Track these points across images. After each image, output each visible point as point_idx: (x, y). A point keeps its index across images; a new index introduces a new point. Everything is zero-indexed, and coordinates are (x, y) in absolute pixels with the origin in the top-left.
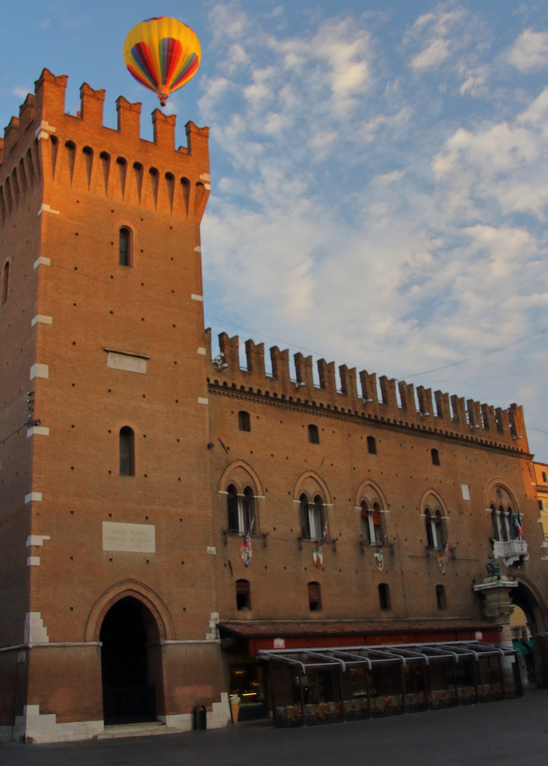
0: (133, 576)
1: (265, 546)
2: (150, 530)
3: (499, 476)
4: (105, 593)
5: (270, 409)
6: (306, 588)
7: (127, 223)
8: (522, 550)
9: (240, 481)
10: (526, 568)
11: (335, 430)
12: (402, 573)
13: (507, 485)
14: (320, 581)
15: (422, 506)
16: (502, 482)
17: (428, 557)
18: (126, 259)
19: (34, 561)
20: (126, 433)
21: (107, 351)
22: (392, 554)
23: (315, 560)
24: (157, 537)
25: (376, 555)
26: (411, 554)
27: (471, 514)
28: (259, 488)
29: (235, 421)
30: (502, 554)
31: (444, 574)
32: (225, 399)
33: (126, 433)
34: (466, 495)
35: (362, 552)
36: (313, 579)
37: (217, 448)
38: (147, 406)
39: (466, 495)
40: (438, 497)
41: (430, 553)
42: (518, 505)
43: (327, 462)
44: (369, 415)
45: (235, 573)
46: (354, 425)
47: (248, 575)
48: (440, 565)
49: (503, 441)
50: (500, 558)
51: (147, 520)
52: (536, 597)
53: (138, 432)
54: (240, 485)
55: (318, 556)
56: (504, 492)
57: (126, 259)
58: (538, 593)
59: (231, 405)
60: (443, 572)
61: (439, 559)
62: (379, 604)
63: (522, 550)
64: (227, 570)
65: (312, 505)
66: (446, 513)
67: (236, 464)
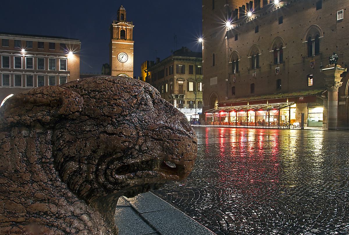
4: (210, 95)
12: (289, 73)
14: (254, 83)
20: (214, 55)
23: (253, 76)
31: (313, 68)
33: (214, 55)
36: (252, 83)
43: (261, 38)
48: (311, 64)
51: (216, 76)
53: (215, 54)
55: (254, 74)
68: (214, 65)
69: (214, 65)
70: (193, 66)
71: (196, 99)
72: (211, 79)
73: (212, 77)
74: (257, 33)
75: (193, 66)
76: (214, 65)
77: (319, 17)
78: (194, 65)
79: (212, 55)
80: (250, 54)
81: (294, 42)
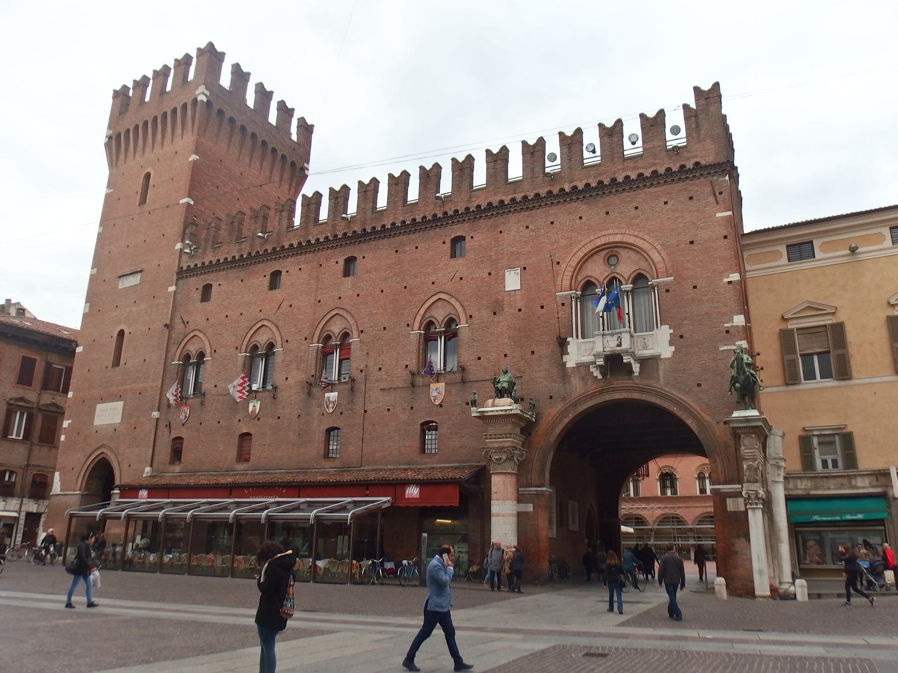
0: (105, 442)
1: (202, 404)
2: (120, 404)
3: (610, 231)
4: (90, 456)
5: (232, 273)
6: (236, 440)
7: (149, 170)
8: (619, 345)
9: (193, 349)
10: (661, 373)
11: (302, 266)
12: (366, 411)
13: (631, 240)
14: (252, 431)
15: (419, 318)
16: (618, 238)
17: (413, 385)
18: (143, 201)
19: (63, 438)
20: (122, 333)
21: (120, 277)
22: (352, 390)
24: (124, 410)
25: (327, 395)
26: (384, 385)
27: (520, 310)
28: (208, 351)
29: (198, 296)
30: (591, 358)
31: (441, 405)
32: (192, 280)
33: (122, 333)
34: (512, 281)
35: (309, 394)
36: (245, 431)
37: (178, 325)
38: (135, 309)
39: (512, 281)
40: (453, 301)
41: (419, 381)
42: (660, 266)
43: (285, 305)
44: (355, 232)
45: (172, 432)
46: (329, 251)
47: (184, 433)
49: (635, 168)
50: (583, 367)
51: (120, 398)
52: (689, 422)
54: (194, 353)
56: (623, 254)
57: (143, 201)
58: (694, 416)
59: (195, 284)
60: (437, 403)
61: (433, 386)
62: (322, 452)
63: (619, 345)
64: (166, 430)
65: (261, 354)
66: (463, 318)
67: (191, 335)
68: (118, 365)
69: (116, 362)
70: (36, 360)
71: (28, 465)
72: (100, 407)
73: (102, 400)
74: (273, 291)
75: (36, 360)
76: (116, 362)
77: (458, 275)
78: (38, 358)
79: (115, 335)
80: (244, 347)
81: (385, 328)
